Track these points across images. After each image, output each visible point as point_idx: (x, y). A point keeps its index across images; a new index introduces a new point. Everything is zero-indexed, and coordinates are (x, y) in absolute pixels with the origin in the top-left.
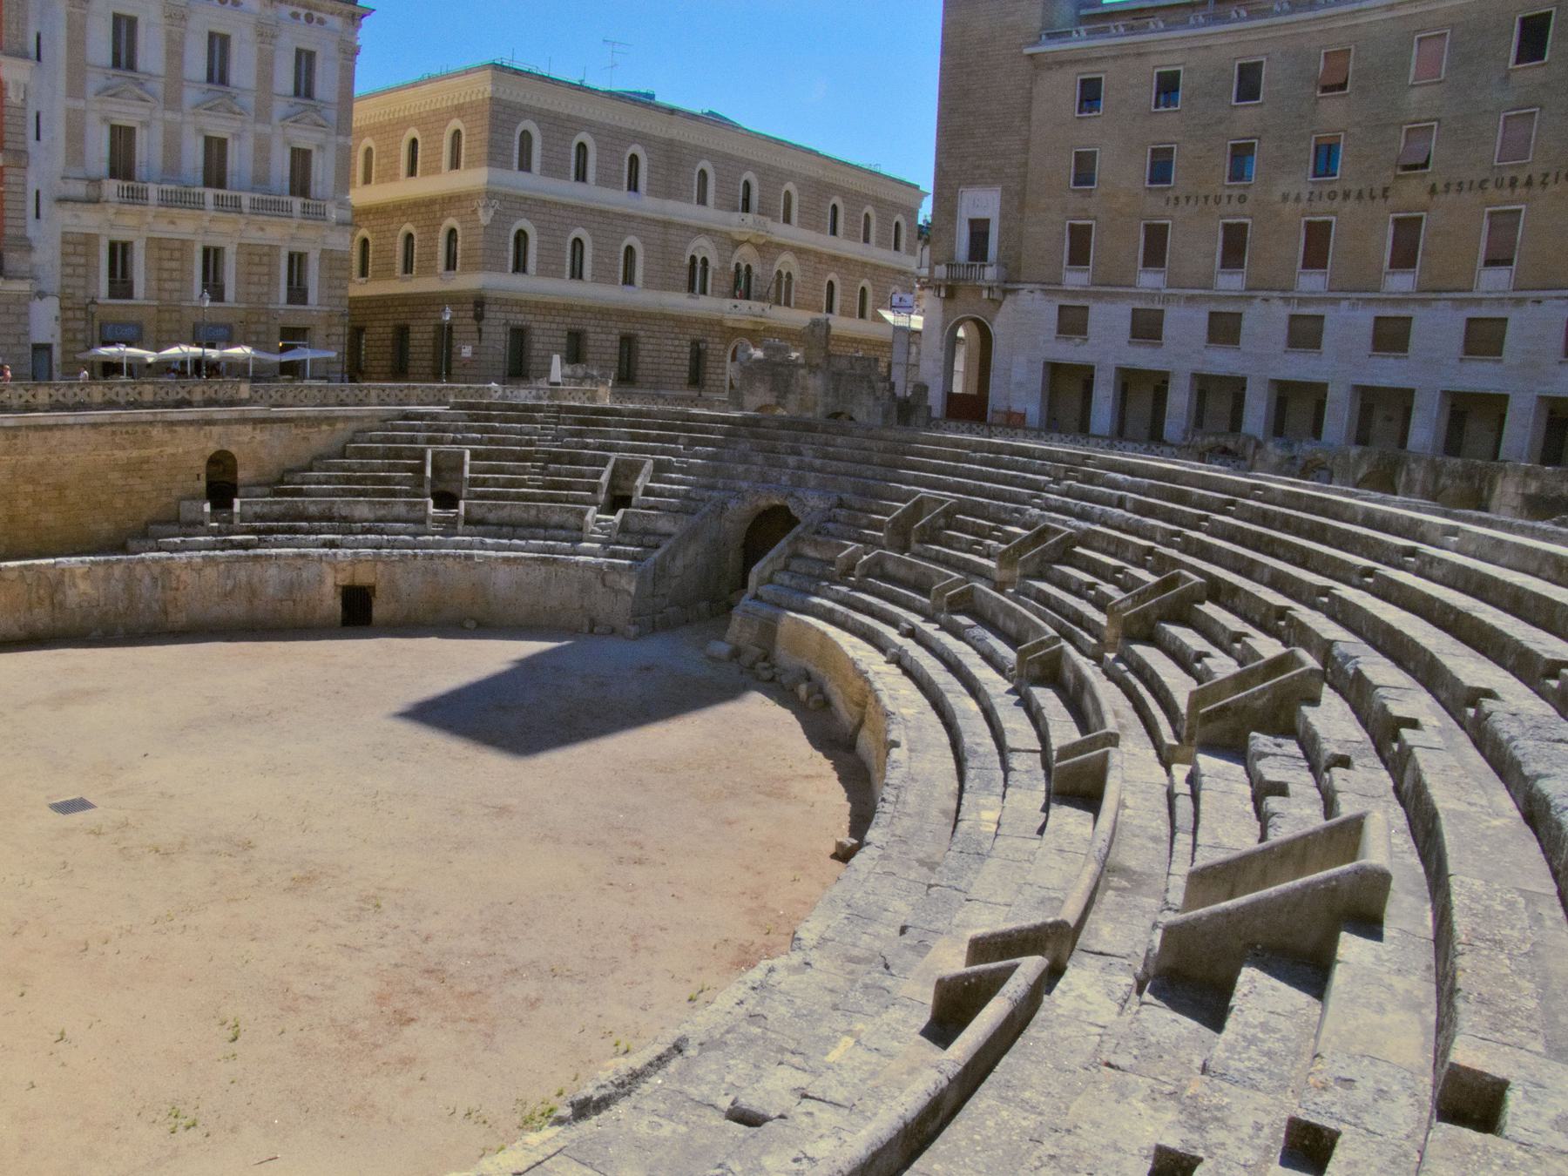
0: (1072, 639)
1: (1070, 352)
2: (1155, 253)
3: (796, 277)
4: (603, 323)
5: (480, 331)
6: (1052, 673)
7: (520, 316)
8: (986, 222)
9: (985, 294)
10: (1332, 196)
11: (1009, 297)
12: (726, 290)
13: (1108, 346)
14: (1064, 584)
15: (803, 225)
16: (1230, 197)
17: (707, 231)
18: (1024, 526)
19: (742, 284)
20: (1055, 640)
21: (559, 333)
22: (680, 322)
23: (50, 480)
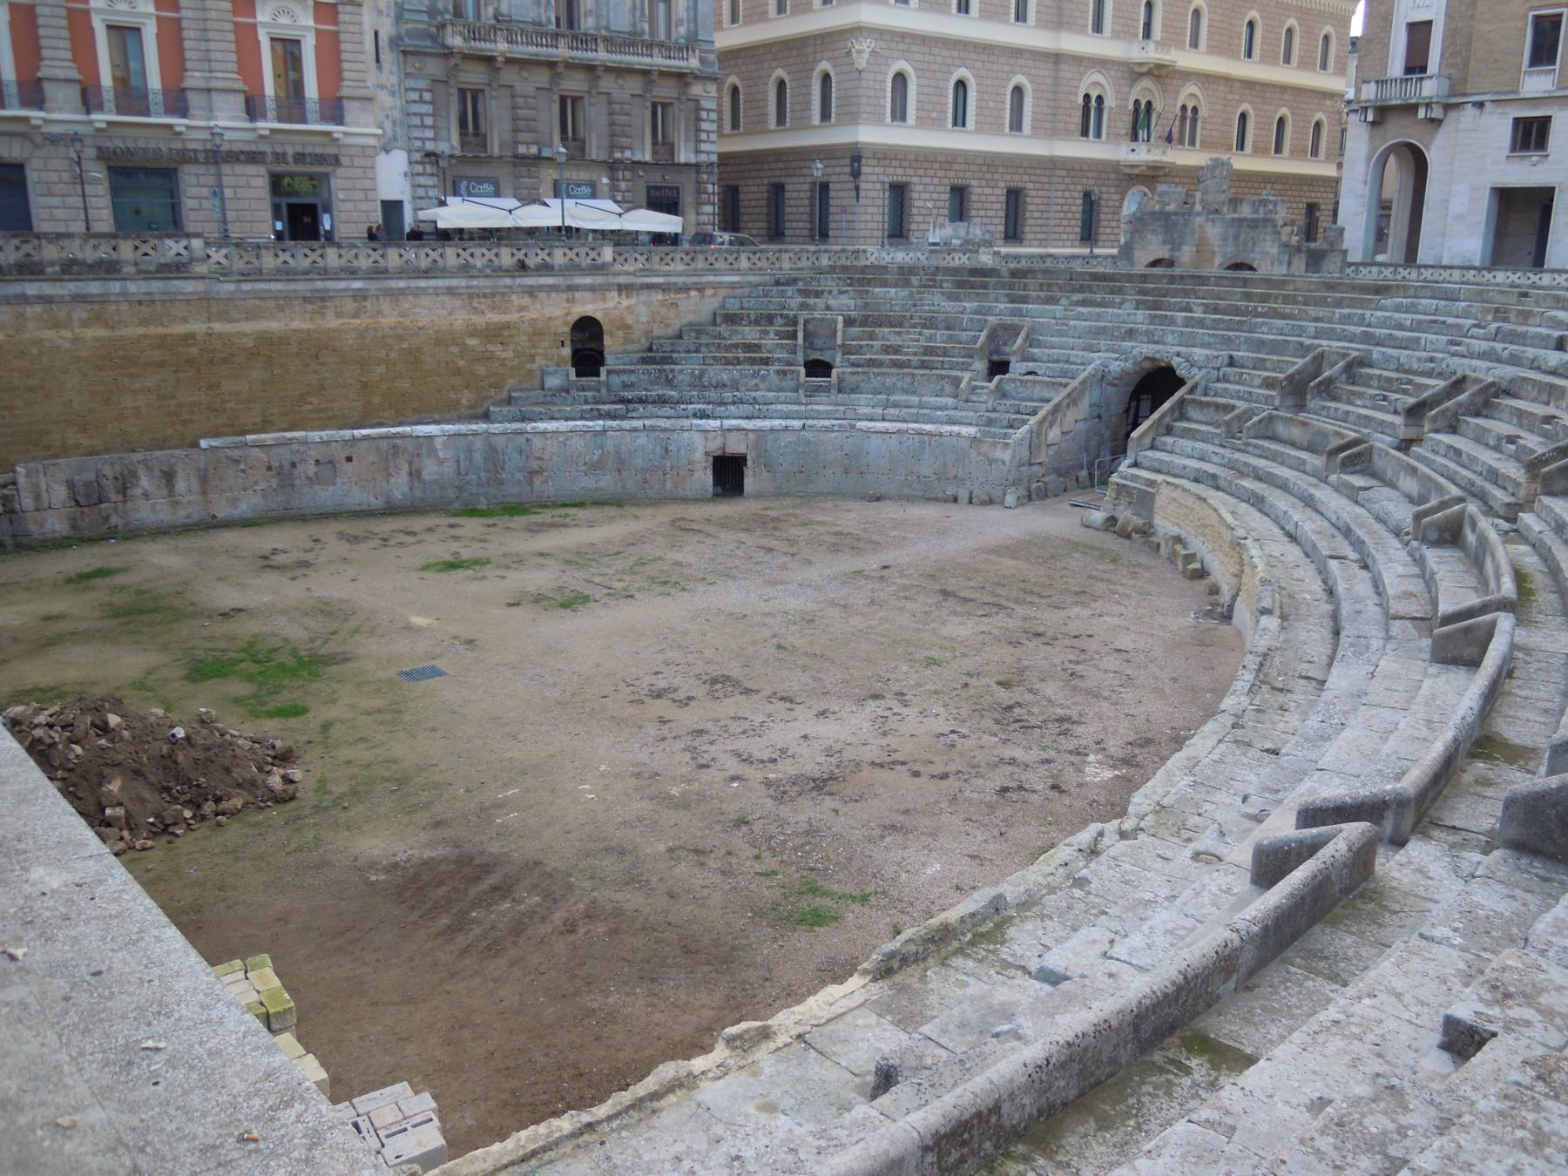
0: (1481, 497)
1: (1525, 173)
3: (1202, 113)
4: (989, 176)
5: (857, 188)
6: (1451, 535)
7: (900, 171)
9: (1421, 113)
11: (1453, 114)
12: (1123, 132)
14: (1480, 438)
15: (1214, 50)
17: (1101, 63)
18: (1440, 375)
19: (1140, 120)
20: (1461, 500)
21: (940, 189)
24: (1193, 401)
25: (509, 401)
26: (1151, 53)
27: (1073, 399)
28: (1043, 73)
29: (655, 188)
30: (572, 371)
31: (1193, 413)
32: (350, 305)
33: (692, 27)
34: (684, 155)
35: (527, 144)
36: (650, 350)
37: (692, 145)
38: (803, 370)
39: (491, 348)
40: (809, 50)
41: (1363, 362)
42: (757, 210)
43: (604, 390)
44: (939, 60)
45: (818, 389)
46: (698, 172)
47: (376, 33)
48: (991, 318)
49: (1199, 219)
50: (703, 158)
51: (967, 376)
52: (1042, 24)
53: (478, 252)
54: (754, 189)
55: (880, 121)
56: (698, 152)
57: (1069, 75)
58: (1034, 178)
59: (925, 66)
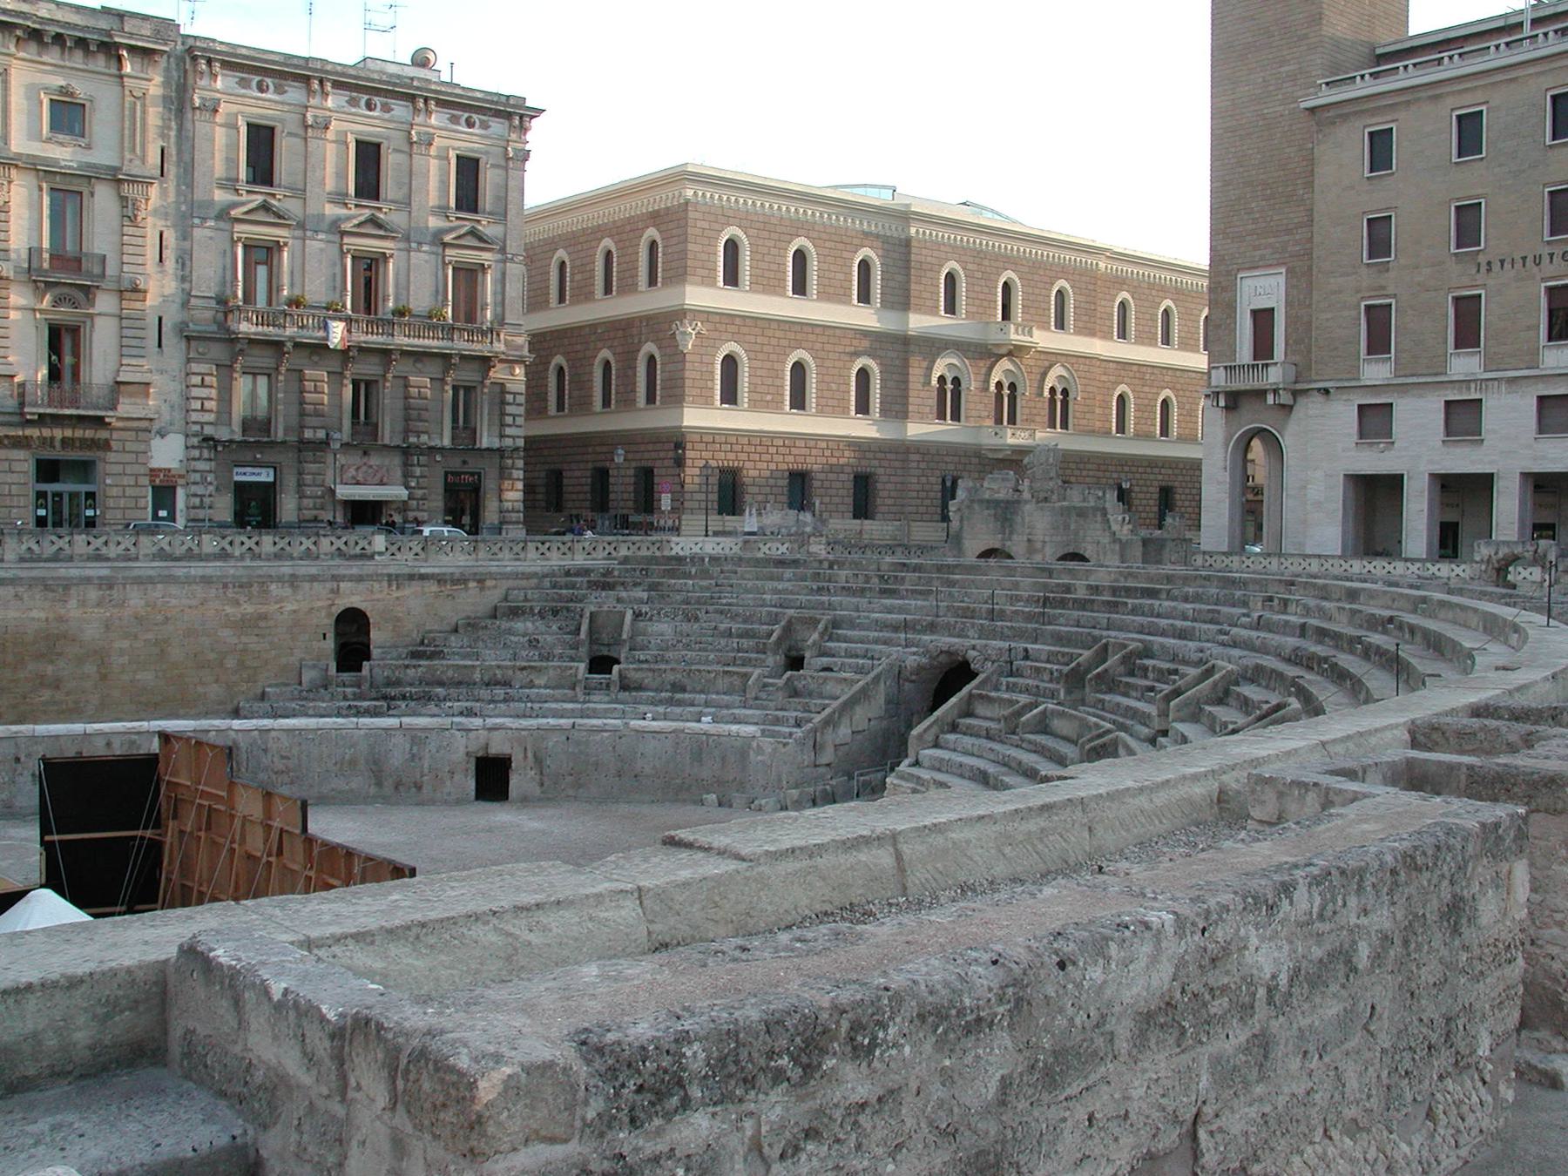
7: (731, 456)
9: (1270, 399)
11: (1302, 401)
13: (1419, 449)
15: (1079, 331)
16: (1551, 255)
23: (150, 636)
24: (981, 697)
25: (263, 696)
27: (863, 695)
28: (890, 354)
29: (452, 473)
30: (333, 666)
31: (980, 709)
32: (93, 594)
33: (499, 309)
34: (485, 441)
35: (314, 428)
36: (422, 643)
37: (496, 430)
38: (582, 666)
39: (244, 639)
40: (635, 331)
41: (1147, 652)
42: (581, 496)
43: (365, 687)
44: (774, 341)
45: (599, 687)
46: (502, 457)
47: (160, 319)
48: (791, 612)
50: (508, 442)
51: (757, 671)
53: (238, 539)
54: (577, 473)
55: (707, 402)
56: (502, 436)
59: (758, 348)
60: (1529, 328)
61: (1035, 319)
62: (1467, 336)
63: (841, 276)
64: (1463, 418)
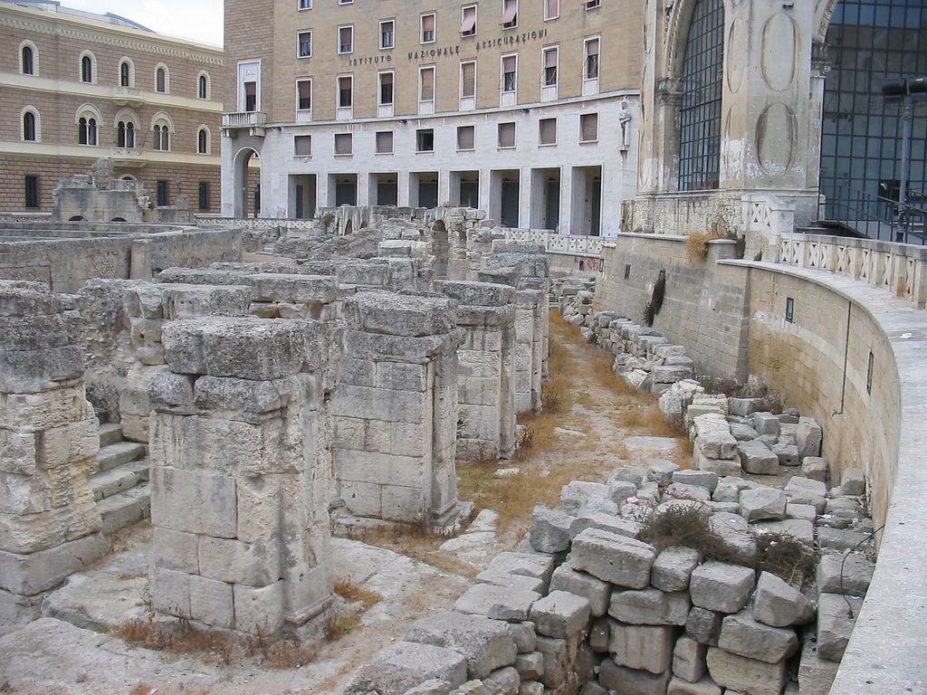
1: (303, 168)
2: (345, 99)
3: (171, 129)
4: (11, 167)
8: (255, 83)
10: (433, 53)
11: (269, 134)
13: (324, 162)
15: (175, 93)
19: (123, 136)
22: (190, 169)
26: (123, 94)
49: (94, 192)
52: (44, 74)
57: (68, 107)
58: (46, 169)
60: (373, 96)
61: (144, 85)
62: (345, 99)
63: (12, 57)
64: (343, 142)
